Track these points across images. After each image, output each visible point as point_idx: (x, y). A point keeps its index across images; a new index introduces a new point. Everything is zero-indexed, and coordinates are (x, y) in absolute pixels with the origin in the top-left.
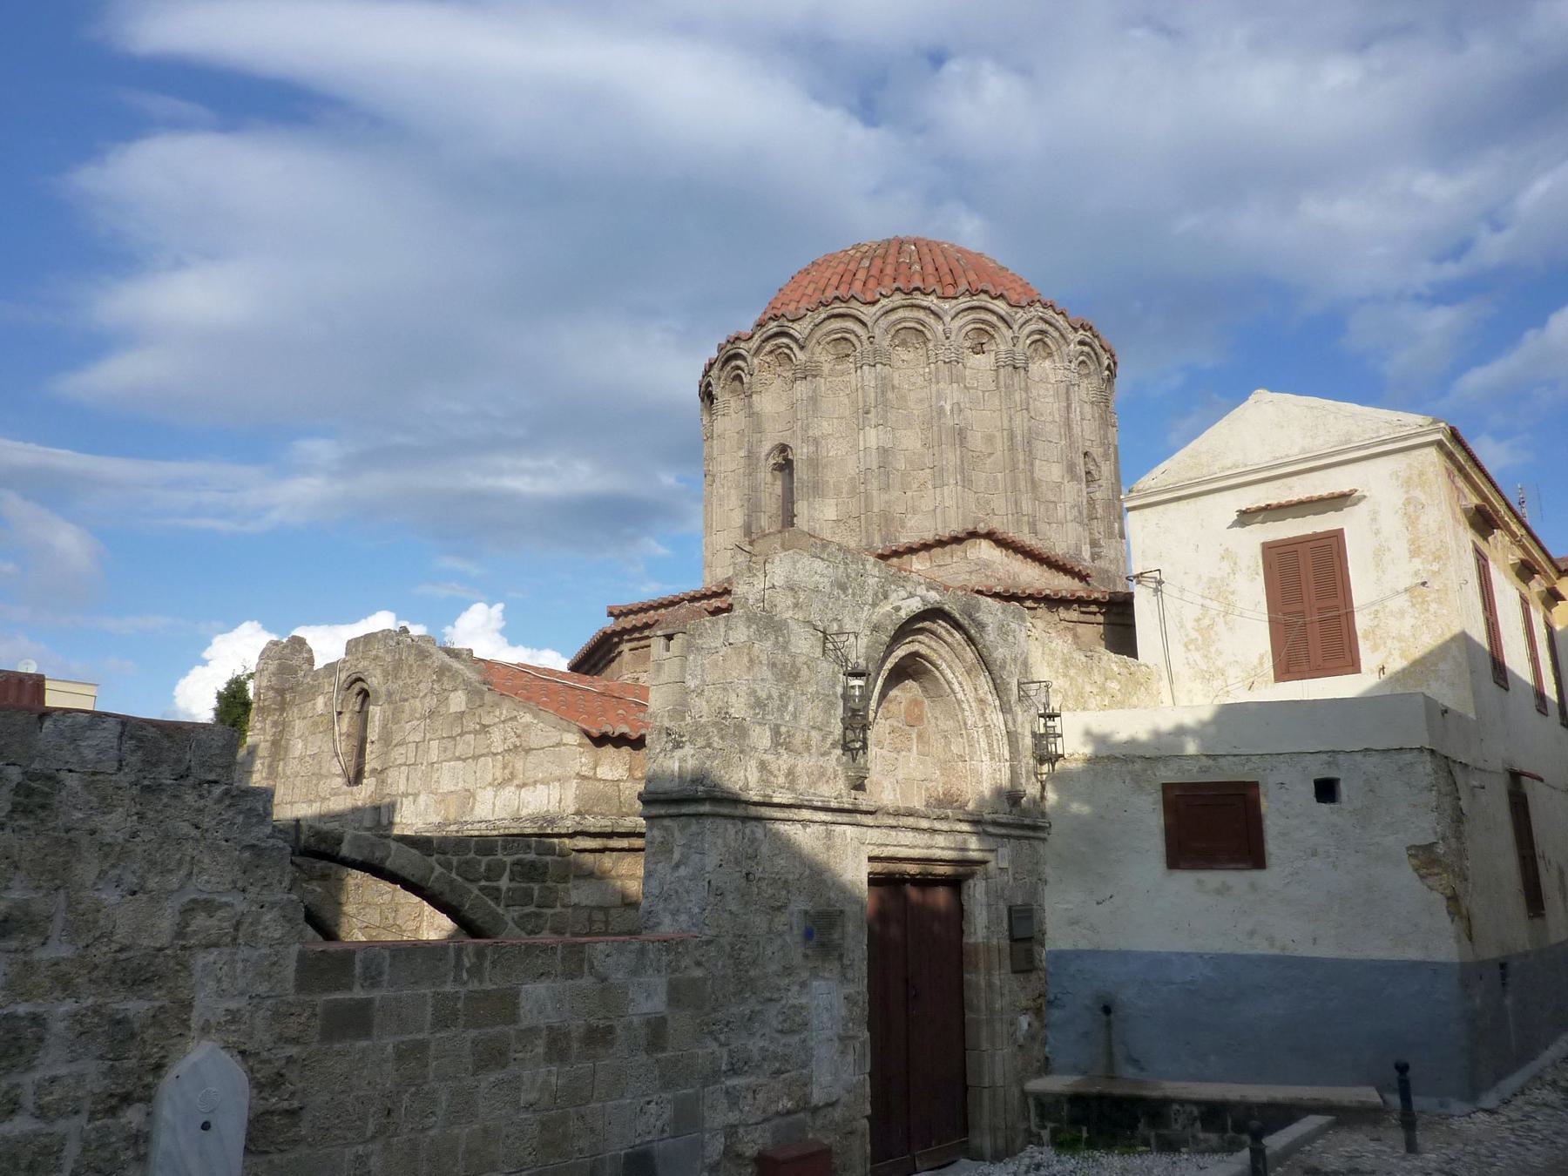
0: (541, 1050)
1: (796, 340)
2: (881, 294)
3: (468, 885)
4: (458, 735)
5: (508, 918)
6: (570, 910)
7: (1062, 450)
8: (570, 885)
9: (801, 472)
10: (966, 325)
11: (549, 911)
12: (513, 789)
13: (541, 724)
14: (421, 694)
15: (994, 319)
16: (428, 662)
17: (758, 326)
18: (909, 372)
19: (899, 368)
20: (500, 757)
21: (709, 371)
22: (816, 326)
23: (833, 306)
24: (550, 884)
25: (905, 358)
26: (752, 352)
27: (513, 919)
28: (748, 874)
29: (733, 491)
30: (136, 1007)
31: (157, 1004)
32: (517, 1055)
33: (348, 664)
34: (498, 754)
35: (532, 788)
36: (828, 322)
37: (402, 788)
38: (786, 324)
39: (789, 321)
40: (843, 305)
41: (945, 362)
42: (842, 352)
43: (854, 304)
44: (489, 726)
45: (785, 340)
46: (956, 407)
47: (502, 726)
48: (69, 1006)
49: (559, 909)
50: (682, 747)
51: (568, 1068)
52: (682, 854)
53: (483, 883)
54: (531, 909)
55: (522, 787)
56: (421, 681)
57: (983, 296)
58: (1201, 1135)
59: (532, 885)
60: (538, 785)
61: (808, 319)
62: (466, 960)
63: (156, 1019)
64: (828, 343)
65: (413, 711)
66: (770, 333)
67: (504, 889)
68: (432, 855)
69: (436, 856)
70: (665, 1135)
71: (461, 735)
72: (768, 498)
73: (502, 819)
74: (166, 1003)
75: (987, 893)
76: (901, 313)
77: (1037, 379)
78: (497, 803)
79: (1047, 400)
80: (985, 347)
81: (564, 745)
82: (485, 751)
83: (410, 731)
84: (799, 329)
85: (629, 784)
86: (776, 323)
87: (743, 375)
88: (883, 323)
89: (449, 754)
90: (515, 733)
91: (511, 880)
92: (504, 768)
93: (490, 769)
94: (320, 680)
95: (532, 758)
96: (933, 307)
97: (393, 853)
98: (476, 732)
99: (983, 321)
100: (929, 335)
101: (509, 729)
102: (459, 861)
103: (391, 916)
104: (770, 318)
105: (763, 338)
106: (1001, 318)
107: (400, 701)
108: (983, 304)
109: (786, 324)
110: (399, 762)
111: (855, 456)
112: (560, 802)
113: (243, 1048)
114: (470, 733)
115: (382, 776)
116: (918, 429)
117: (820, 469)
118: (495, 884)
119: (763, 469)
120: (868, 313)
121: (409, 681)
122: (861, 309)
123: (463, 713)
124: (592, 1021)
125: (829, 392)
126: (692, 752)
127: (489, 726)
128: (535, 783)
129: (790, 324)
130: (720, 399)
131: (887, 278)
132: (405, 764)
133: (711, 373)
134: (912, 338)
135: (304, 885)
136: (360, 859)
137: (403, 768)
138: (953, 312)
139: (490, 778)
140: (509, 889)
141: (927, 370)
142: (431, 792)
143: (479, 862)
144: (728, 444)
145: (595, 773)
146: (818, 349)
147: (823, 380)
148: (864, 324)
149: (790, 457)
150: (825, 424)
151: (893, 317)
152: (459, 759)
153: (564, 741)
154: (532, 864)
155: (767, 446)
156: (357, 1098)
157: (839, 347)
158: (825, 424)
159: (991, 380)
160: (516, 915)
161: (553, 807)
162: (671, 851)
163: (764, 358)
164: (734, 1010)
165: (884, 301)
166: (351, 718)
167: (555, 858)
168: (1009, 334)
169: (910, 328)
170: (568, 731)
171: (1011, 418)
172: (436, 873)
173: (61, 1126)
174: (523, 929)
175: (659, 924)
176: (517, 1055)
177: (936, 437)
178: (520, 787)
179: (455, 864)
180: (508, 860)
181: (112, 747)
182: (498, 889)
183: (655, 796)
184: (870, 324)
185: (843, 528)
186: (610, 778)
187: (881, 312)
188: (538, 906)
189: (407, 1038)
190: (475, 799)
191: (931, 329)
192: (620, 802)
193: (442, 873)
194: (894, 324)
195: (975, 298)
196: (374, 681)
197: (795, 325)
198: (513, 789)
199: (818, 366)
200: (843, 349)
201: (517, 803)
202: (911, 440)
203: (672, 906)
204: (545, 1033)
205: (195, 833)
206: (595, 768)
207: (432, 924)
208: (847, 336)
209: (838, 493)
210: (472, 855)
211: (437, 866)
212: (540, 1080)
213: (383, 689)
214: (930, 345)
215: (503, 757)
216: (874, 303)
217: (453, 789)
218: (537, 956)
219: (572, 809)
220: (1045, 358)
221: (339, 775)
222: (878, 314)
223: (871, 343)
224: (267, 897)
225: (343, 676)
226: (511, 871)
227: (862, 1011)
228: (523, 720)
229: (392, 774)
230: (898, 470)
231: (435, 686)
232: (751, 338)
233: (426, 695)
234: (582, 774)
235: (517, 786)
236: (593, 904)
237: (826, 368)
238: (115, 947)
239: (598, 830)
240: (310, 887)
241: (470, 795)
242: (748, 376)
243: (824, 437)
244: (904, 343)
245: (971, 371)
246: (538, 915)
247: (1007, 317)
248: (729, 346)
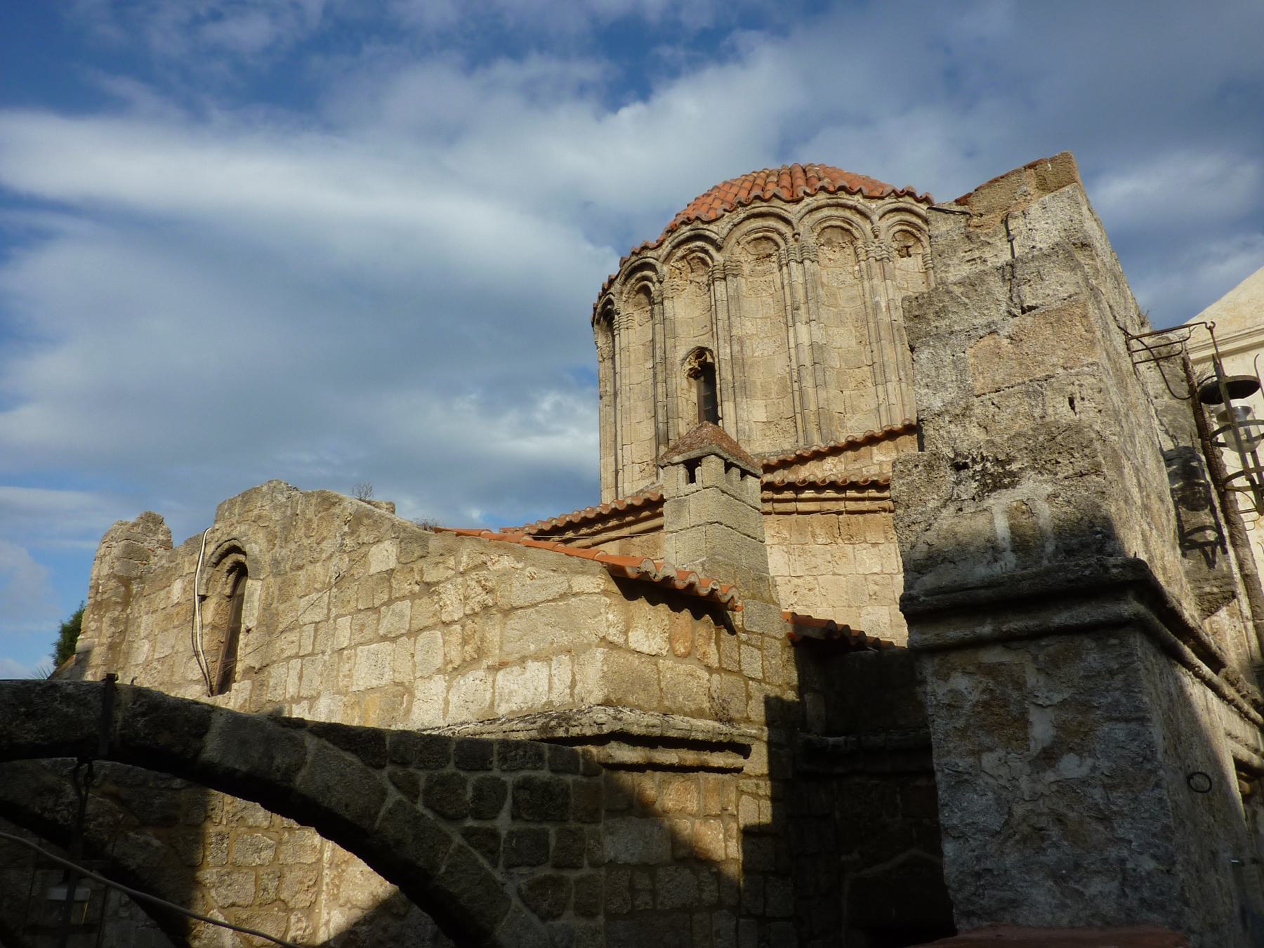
1: (712, 242)
2: (805, 193)
3: (445, 827)
4: (383, 605)
5: (510, 889)
6: (603, 872)
8: (601, 827)
9: (724, 374)
11: (573, 875)
12: (481, 673)
13: (531, 569)
14: (324, 556)
15: (919, 222)
16: (337, 510)
17: (668, 232)
18: (837, 270)
19: (825, 267)
20: (457, 627)
21: (609, 287)
22: (735, 225)
23: (753, 205)
24: (573, 825)
25: (831, 257)
26: (662, 259)
27: (519, 890)
29: (640, 404)
33: (218, 534)
35: (517, 669)
36: (747, 222)
37: (292, 691)
38: (701, 226)
39: (704, 222)
40: (765, 204)
41: (876, 260)
42: (763, 253)
43: (777, 202)
44: (438, 583)
45: (699, 243)
47: (460, 580)
49: (586, 871)
50: (1013, 485)
52: (1061, 727)
53: (470, 823)
54: (545, 871)
55: (498, 670)
56: (324, 538)
57: (908, 199)
59: (546, 826)
60: (530, 665)
61: (726, 219)
64: (749, 243)
66: (682, 237)
67: (504, 833)
68: (382, 767)
69: (389, 768)
72: (685, 404)
73: (462, 724)
76: (826, 212)
78: (453, 699)
82: (430, 622)
83: (307, 609)
84: (715, 231)
86: (689, 227)
87: (650, 284)
88: (809, 220)
89: (368, 633)
90: (484, 587)
91: (514, 818)
92: (465, 642)
94: (179, 560)
95: (515, 622)
96: (859, 207)
97: (309, 758)
98: (413, 596)
99: (909, 224)
100: (856, 234)
101: (474, 583)
102: (429, 779)
103: (272, 885)
104: (683, 223)
105: (673, 243)
107: (292, 570)
108: (908, 206)
109: (701, 226)
111: (785, 356)
112: (573, 684)
114: (404, 598)
115: (261, 677)
116: (852, 328)
117: (747, 368)
118: (487, 825)
119: (678, 374)
120: (793, 211)
121: (305, 542)
122: (784, 207)
123: (393, 570)
125: (751, 292)
126: (1049, 489)
127: (438, 583)
128: (523, 660)
129: (705, 226)
130: (622, 313)
132: (297, 656)
133: (612, 290)
134: (837, 237)
135: (131, 834)
136: (244, 768)
137: (293, 662)
138: (880, 212)
139: (439, 661)
140: (511, 834)
141: (857, 268)
142: (339, 693)
143: (463, 782)
144: (632, 357)
145: (626, 640)
146: (738, 249)
147: (744, 280)
148: (788, 222)
149: (709, 360)
150: (748, 324)
151: (818, 215)
152: (384, 638)
153: (576, 589)
154: (546, 786)
155: (682, 352)
157: (760, 247)
158: (748, 324)
160: (522, 883)
161: (560, 696)
162: (1023, 722)
163: (675, 265)
165: (808, 200)
166: (219, 604)
167: (579, 778)
169: (836, 227)
170: (583, 573)
172: (390, 802)
174: (534, 911)
175: (1015, 903)
177: (873, 334)
178: (494, 669)
179: (422, 784)
180: (509, 779)
182: (494, 835)
183: (959, 596)
184: (795, 221)
185: (774, 429)
186: (645, 649)
187: (807, 209)
188: (557, 866)
190: (412, 695)
192: (661, 690)
193: (399, 803)
194: (820, 222)
195: (901, 199)
196: (256, 547)
197: (712, 227)
198: (481, 673)
199: (738, 265)
200: (764, 249)
201: (488, 696)
202: (844, 339)
203: (1051, 856)
206: (626, 633)
207: (336, 897)
208: (770, 234)
209: (767, 395)
210: (450, 769)
211: (391, 789)
213: (267, 558)
215: (463, 626)
216: (798, 201)
217: (375, 683)
219: (598, 696)
221: (197, 682)
222: (803, 211)
223: (796, 240)
225: (211, 548)
226: (515, 802)
228: (497, 566)
229: (277, 672)
230: (833, 368)
231: (347, 541)
232: (660, 245)
233: (331, 555)
234: (610, 638)
235: (489, 668)
236: (635, 860)
237: (746, 268)
239: (643, 731)
240: (142, 839)
241: (404, 690)
242: (657, 285)
243: (750, 337)
244: (829, 242)
245: (900, 272)
246: (557, 883)
248: (634, 258)
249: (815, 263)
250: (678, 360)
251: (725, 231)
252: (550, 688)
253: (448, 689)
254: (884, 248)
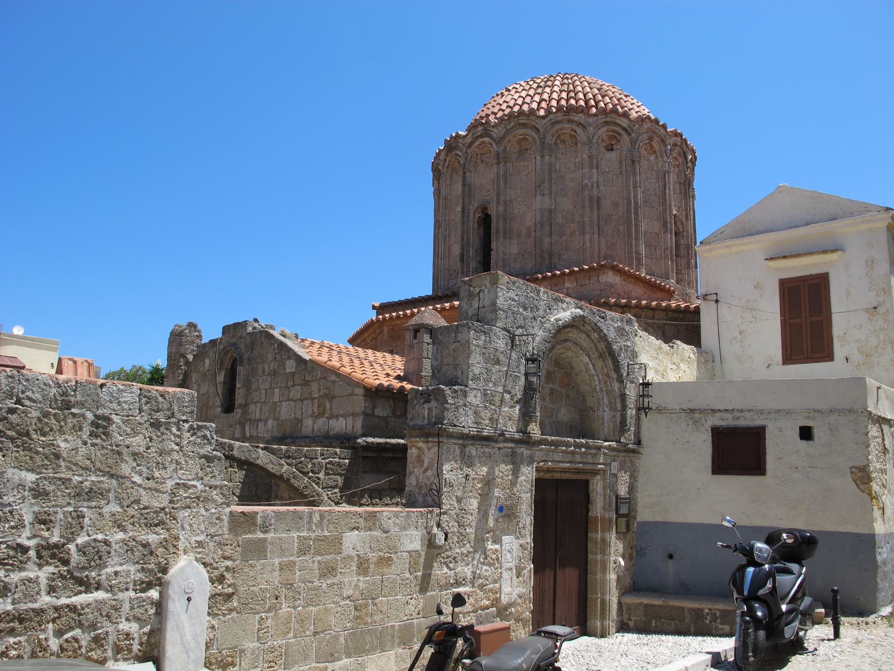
0: (354, 568)
7: (660, 212)
12: (324, 419)
13: (341, 383)
15: (621, 131)
20: (316, 400)
26: (467, 145)
28: (467, 475)
30: (153, 538)
31: (162, 536)
32: (341, 570)
34: (315, 398)
37: (258, 416)
40: (525, 118)
44: (310, 381)
48: (121, 535)
51: (368, 578)
52: (429, 463)
56: (268, 353)
58: (720, 627)
60: (340, 418)
62: (314, 519)
63: (164, 544)
65: (264, 370)
70: (420, 616)
71: (293, 386)
73: (318, 437)
74: (167, 536)
75: (604, 488)
81: (356, 395)
82: (308, 396)
85: (393, 419)
92: (319, 406)
93: (309, 408)
99: (613, 131)
106: (624, 129)
110: (255, 400)
113: (204, 560)
114: (298, 385)
122: (537, 121)
124: (381, 554)
126: (436, 405)
127: (310, 381)
131: (553, 101)
132: (259, 402)
136: (244, 458)
139: (310, 412)
142: (276, 419)
145: (373, 412)
152: (292, 400)
153: (355, 393)
155: (475, 205)
156: (261, 589)
159: (617, 168)
162: (423, 462)
164: (458, 550)
166: (226, 373)
170: (358, 387)
172: (285, 468)
173: (120, 596)
176: (341, 570)
178: (329, 418)
181: (136, 402)
189: (285, 559)
192: (388, 429)
198: (324, 419)
201: (327, 428)
204: (356, 559)
205: (177, 448)
207: (277, 495)
212: (353, 584)
215: (319, 400)
218: (352, 518)
220: (651, 154)
221: (219, 407)
224: (213, 482)
227: (529, 553)
229: (252, 407)
230: (557, 224)
231: (277, 356)
235: (327, 417)
238: (142, 506)
247: (628, 129)
250: (472, 211)
251: (502, 134)
252: (346, 427)
253: (314, 423)
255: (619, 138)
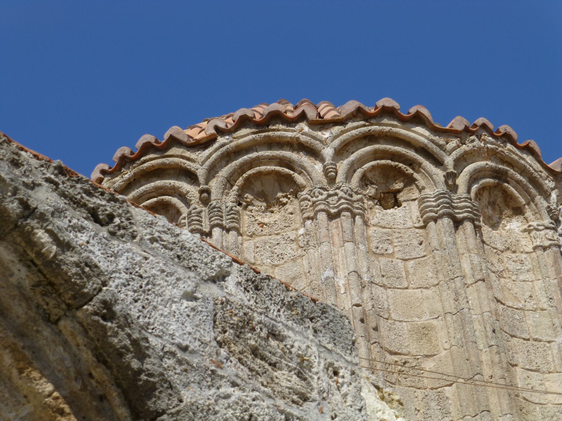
10: (361, 161)
15: (412, 153)
25: (266, 220)
46: (353, 277)
77: (500, 247)
79: (522, 277)
80: (401, 197)
96: (303, 138)
99: (394, 156)
100: (300, 179)
141: (302, 231)
148: (191, 177)
159: (415, 242)
165: (221, 140)
168: (439, 174)
171: (457, 294)
184: (201, 172)
191: (302, 170)
214: (304, 194)
249: (233, 233)
254: (341, 194)
255: (410, 171)
